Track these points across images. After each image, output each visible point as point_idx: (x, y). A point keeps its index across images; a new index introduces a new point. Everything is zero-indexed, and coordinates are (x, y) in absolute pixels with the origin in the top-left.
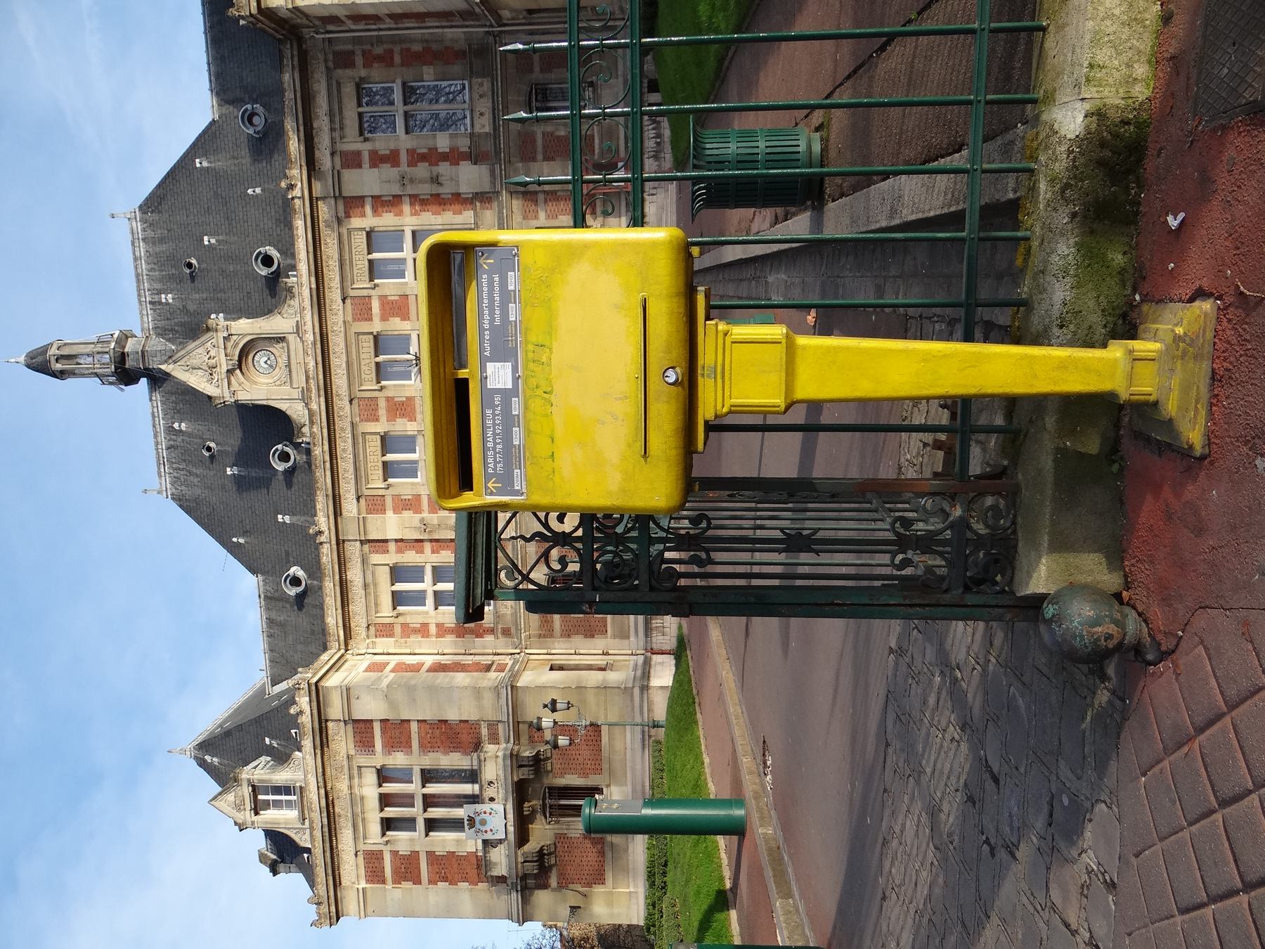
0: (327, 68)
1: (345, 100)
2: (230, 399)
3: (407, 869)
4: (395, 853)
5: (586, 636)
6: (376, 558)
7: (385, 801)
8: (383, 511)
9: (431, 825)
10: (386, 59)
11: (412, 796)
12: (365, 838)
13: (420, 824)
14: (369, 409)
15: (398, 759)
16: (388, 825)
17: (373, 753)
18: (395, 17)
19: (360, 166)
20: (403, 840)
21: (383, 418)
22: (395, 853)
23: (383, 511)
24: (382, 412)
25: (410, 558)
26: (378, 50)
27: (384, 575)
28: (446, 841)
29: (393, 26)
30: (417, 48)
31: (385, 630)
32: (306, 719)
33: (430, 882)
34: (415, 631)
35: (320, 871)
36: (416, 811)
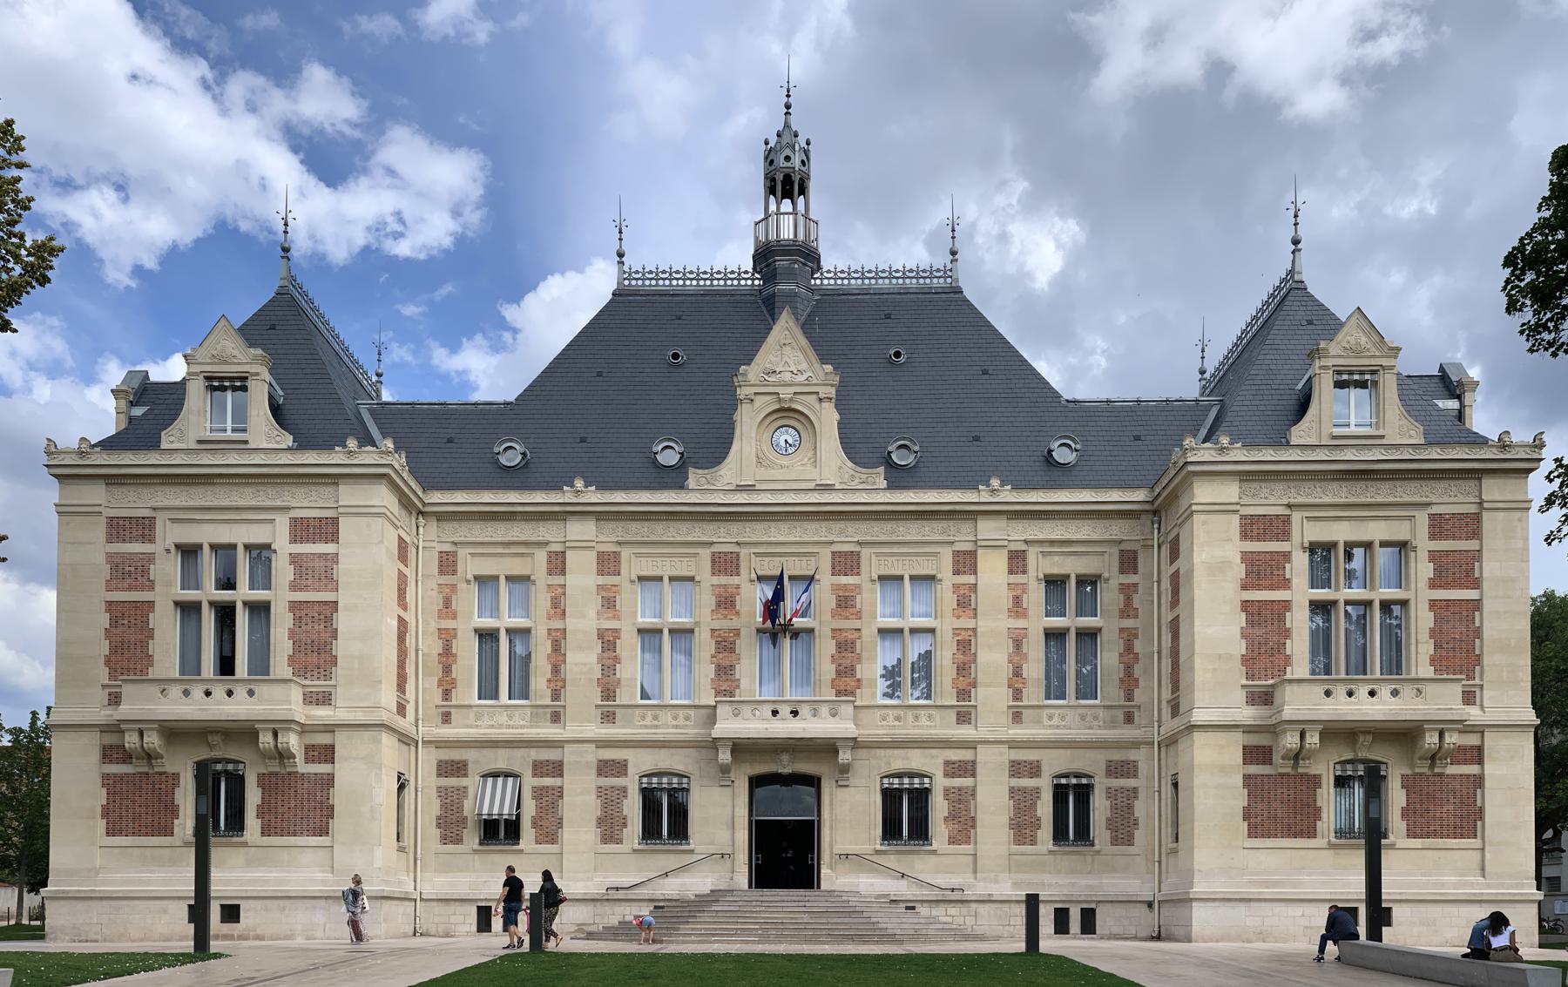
0: (1121, 542)
1: (1084, 559)
2: (742, 392)
3: (131, 572)
4: (150, 558)
5: (438, 818)
6: (541, 556)
7: (225, 551)
8: (601, 572)
9: (189, 610)
10: (1127, 611)
11: (228, 583)
12: (173, 520)
13: (191, 595)
14: (725, 563)
15: (283, 571)
16: (189, 552)
17: (294, 540)
18: (1175, 625)
19: (1011, 572)
20: (168, 569)
21: (716, 580)
22: (150, 558)
23: (601, 572)
24: (723, 580)
25: (541, 600)
26: (1137, 601)
27: (517, 567)
28: (166, 630)
29: (1163, 621)
30: (1138, 646)
31: (447, 564)
32: (337, 457)
33: (110, 603)
34: (447, 603)
35: (127, 458)
36: (209, 592)
